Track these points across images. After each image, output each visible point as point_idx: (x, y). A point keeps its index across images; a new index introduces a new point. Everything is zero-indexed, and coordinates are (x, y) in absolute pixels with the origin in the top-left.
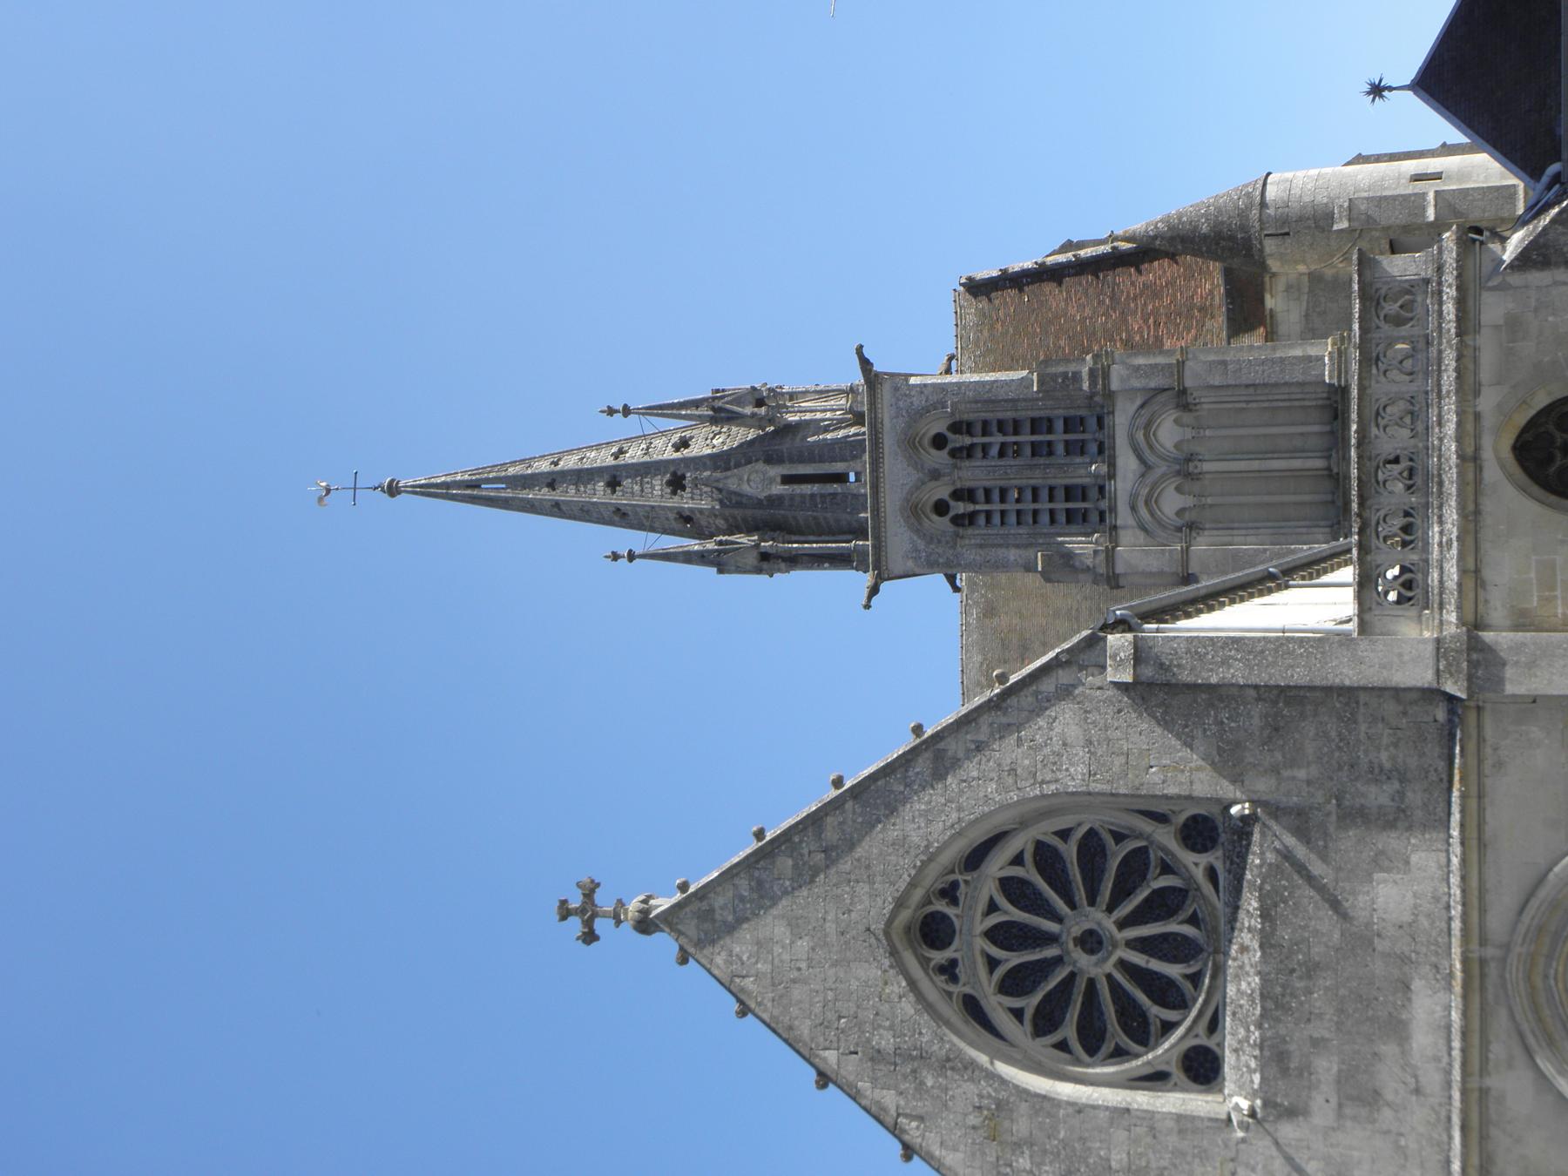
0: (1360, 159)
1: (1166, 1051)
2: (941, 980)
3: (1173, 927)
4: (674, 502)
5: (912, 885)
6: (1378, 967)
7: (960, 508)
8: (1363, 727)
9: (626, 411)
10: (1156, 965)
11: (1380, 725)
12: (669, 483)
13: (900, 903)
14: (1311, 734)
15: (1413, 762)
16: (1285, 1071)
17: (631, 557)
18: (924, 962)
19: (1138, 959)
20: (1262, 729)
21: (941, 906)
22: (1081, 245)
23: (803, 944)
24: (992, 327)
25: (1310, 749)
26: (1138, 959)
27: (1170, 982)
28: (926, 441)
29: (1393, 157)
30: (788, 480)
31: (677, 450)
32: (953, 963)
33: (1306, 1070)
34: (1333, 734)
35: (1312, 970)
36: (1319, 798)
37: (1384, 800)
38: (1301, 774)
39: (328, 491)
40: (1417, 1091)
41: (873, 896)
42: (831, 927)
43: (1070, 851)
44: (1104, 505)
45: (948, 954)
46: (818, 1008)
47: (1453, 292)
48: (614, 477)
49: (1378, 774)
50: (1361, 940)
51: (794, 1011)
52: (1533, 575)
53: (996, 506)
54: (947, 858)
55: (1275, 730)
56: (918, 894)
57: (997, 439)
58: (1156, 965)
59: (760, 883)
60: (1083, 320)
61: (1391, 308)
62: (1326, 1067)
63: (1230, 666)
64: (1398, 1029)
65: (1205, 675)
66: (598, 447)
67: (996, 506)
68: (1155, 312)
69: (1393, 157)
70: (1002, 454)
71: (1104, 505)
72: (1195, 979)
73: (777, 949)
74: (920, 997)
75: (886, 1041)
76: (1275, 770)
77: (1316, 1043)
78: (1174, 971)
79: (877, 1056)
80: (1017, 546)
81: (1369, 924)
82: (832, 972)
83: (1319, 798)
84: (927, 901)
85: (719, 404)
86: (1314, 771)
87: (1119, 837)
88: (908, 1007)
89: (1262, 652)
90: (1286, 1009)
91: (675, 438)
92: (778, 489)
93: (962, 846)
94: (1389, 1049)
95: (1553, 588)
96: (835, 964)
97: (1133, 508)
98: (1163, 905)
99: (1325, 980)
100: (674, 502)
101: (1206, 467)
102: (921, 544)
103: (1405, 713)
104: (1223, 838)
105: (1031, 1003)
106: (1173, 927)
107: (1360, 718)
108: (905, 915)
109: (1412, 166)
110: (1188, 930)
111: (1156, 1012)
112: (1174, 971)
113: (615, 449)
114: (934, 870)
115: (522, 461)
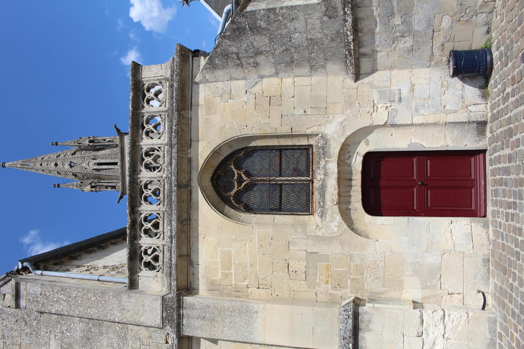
8: (130, 343)
11: (139, 343)
14: (105, 344)
20: (82, 338)
34: (115, 345)
52: (219, 259)
63: (61, 304)
65: (49, 308)
89: (76, 297)
92: (96, 167)
95: (229, 269)
103: (150, 337)
107: (129, 338)
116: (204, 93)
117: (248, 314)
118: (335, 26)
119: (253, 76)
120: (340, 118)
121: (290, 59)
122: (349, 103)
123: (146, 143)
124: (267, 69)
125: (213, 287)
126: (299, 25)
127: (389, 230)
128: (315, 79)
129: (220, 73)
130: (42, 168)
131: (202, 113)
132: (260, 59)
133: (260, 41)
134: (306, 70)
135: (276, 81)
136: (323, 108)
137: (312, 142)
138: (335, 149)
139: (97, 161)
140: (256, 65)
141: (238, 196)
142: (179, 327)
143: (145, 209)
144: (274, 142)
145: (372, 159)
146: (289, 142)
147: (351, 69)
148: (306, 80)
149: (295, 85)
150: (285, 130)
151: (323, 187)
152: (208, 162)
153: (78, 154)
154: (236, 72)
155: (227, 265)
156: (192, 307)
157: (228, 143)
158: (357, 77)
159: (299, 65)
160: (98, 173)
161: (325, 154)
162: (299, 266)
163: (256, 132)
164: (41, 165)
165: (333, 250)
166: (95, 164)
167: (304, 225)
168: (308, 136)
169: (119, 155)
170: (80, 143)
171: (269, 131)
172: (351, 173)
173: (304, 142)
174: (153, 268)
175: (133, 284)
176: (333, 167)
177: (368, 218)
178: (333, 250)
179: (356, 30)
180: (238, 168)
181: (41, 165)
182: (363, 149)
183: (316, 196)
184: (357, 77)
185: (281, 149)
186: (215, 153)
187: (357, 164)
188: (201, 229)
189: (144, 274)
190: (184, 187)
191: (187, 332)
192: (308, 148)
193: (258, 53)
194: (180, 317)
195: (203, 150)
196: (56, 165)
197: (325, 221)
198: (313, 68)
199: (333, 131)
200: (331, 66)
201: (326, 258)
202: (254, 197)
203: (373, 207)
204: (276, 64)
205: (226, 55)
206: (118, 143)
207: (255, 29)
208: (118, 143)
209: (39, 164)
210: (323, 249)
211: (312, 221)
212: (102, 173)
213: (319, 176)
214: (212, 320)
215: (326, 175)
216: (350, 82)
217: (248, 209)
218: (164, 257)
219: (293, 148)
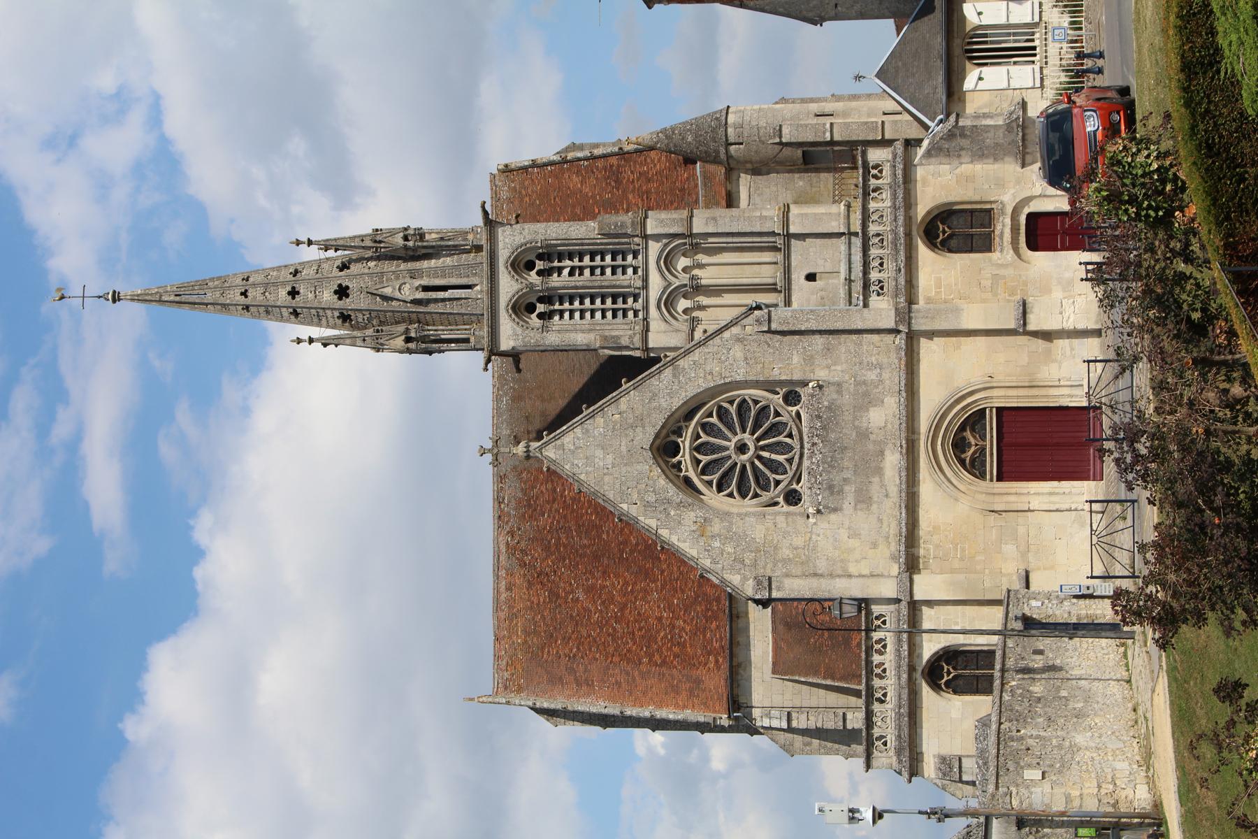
0: (784, 100)
1: (776, 493)
2: (675, 471)
3: (781, 438)
4: (340, 304)
5: (663, 427)
6: (871, 447)
7: (541, 308)
9: (310, 243)
10: (774, 456)
12: (336, 292)
13: (657, 436)
15: (885, 360)
16: (832, 493)
17: (311, 341)
18: (667, 463)
19: (765, 454)
21: (673, 438)
22: (597, 146)
23: (610, 459)
24: (522, 200)
25: (843, 357)
26: (765, 454)
27: (780, 464)
28: (522, 265)
29: (803, 101)
30: (426, 289)
31: (341, 270)
32: (680, 463)
33: (841, 491)
35: (844, 449)
36: (847, 377)
37: (874, 377)
38: (839, 368)
39: (62, 298)
40: (887, 496)
41: (645, 434)
42: (624, 449)
43: (733, 409)
44: (638, 305)
45: (678, 458)
46: (617, 486)
47: (901, 166)
48: (293, 288)
49: (871, 366)
50: (863, 435)
51: (606, 488)
53: (566, 305)
54: (676, 416)
55: (828, 349)
56: (664, 432)
57: (568, 263)
58: (774, 456)
59: (587, 431)
60: (593, 197)
61: (874, 172)
62: (850, 489)
64: (879, 471)
66: (279, 269)
67: (566, 305)
68: (648, 192)
69: (803, 101)
70: (571, 274)
71: (638, 305)
72: (790, 461)
73: (597, 460)
74: (667, 477)
75: (651, 498)
76: (828, 367)
77: (845, 480)
78: (781, 458)
79: (647, 505)
80: (583, 331)
81: (867, 429)
82: (624, 469)
83: (847, 377)
84: (668, 436)
85: (378, 238)
86: (844, 366)
87: (756, 402)
88: (662, 481)
90: (833, 467)
91: (338, 263)
92: (420, 295)
93: (686, 410)
94: (876, 480)
96: (626, 465)
97: (659, 307)
98: (775, 429)
99: (849, 454)
100: (340, 304)
101: (704, 282)
102: (519, 330)
104: (803, 399)
105: (715, 478)
106: (781, 438)
108: (658, 442)
109: (814, 107)
110: (788, 440)
111: (772, 476)
112: (781, 458)
113: (292, 270)
114: (672, 420)
115: (219, 278)
116: (920, 172)
117: (957, 311)
118: (1012, 136)
119: (956, 162)
120: (1012, 191)
121: (982, 153)
122: (1018, 182)
123: (873, 205)
124: (966, 159)
125: (929, 300)
126: (991, 135)
127: (1043, 261)
128: (996, 166)
129: (933, 160)
130: (248, 301)
131: (919, 185)
132: (963, 153)
133: (965, 142)
134: (991, 160)
135: (971, 166)
136: (1001, 184)
137: (993, 206)
138: (1009, 210)
139: (425, 282)
140: (959, 156)
141: (943, 243)
142: (909, 324)
143: (874, 252)
144: (969, 207)
145: (1031, 216)
146: (978, 206)
147: (1020, 161)
148: (991, 167)
149: (981, 169)
150: (977, 198)
151: (1002, 233)
152: (923, 219)
153: (355, 268)
154: (944, 160)
155: (939, 286)
156: (918, 311)
157: (937, 207)
158: (1023, 166)
159: (987, 157)
160: (421, 309)
161: (1003, 212)
162: (988, 283)
163: (958, 199)
164: (244, 294)
165: (1009, 272)
166: (417, 289)
167: (990, 260)
168: (991, 202)
169: (485, 267)
170: (380, 242)
171: (966, 199)
172: (1019, 225)
173: (988, 206)
174: (879, 295)
175: (866, 305)
176: (1008, 221)
177: (1030, 253)
178: (1009, 272)
179: (1024, 139)
180: (943, 223)
181: (244, 294)
182: (1027, 210)
183: (997, 239)
184: (1023, 166)
185: (972, 211)
186: (929, 213)
187: (1023, 219)
188: (920, 263)
189: (873, 298)
190: (908, 235)
191: (915, 327)
192: (989, 211)
193: (962, 149)
194: (910, 318)
195: (921, 210)
196: (293, 293)
197: (1003, 255)
198: (996, 160)
199: (1008, 199)
200: (1007, 159)
201: (1004, 277)
202: (953, 243)
203: (1033, 245)
204: (973, 156)
205: (940, 149)
206: (483, 242)
207: (963, 135)
208: (483, 242)
209: (238, 291)
210: (1002, 272)
211: (995, 256)
212: (432, 308)
213: (999, 227)
214: (933, 318)
215: (1003, 227)
216: (1018, 169)
217: (950, 251)
218: (889, 286)
219: (982, 211)
